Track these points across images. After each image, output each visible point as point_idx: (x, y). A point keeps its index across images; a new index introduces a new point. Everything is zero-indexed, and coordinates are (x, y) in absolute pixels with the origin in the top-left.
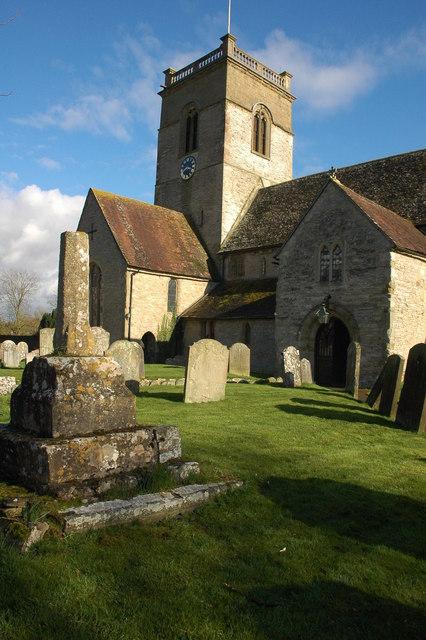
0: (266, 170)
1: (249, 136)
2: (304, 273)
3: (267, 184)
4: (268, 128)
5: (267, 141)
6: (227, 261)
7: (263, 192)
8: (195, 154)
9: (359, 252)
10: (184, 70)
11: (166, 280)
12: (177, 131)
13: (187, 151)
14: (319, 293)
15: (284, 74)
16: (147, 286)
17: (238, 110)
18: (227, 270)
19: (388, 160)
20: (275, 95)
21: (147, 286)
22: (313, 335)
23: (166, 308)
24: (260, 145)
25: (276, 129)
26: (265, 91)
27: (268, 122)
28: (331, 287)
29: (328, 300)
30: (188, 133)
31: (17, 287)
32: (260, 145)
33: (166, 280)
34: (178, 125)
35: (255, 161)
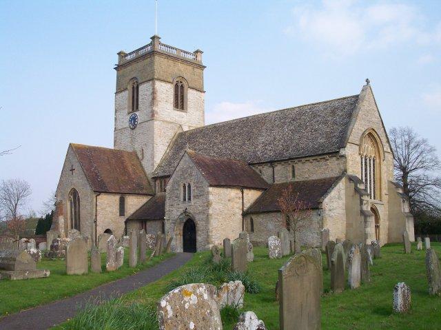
0: (185, 120)
1: (172, 99)
2: (176, 197)
3: (186, 129)
4: (185, 91)
5: (185, 100)
6: (158, 182)
7: (182, 135)
8: (137, 113)
9: (197, 187)
10: (130, 54)
11: (117, 198)
12: (126, 95)
13: (133, 109)
14: (182, 207)
15: (197, 52)
16: (106, 202)
17: (163, 84)
18: (157, 188)
19: (248, 118)
20: (190, 68)
21: (106, 202)
22: (182, 228)
23: (118, 214)
24: (180, 102)
25: (190, 91)
26: (181, 66)
27: (186, 87)
28: (186, 205)
29: (185, 212)
30: (133, 97)
31: (14, 194)
32: (180, 102)
33: (117, 198)
34: (127, 92)
35: (177, 115)
